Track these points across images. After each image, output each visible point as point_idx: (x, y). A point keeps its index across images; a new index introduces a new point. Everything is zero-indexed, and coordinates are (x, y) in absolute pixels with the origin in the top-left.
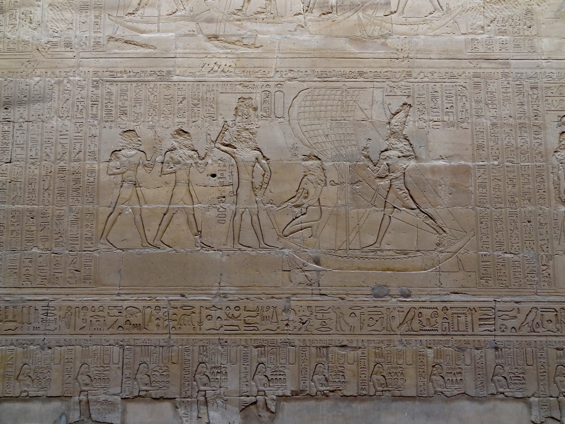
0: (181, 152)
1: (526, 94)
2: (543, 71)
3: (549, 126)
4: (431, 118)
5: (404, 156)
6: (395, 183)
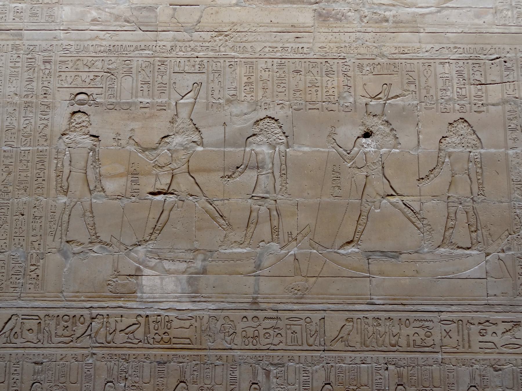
1: (36, 69)
2: (61, 42)
3: (59, 105)
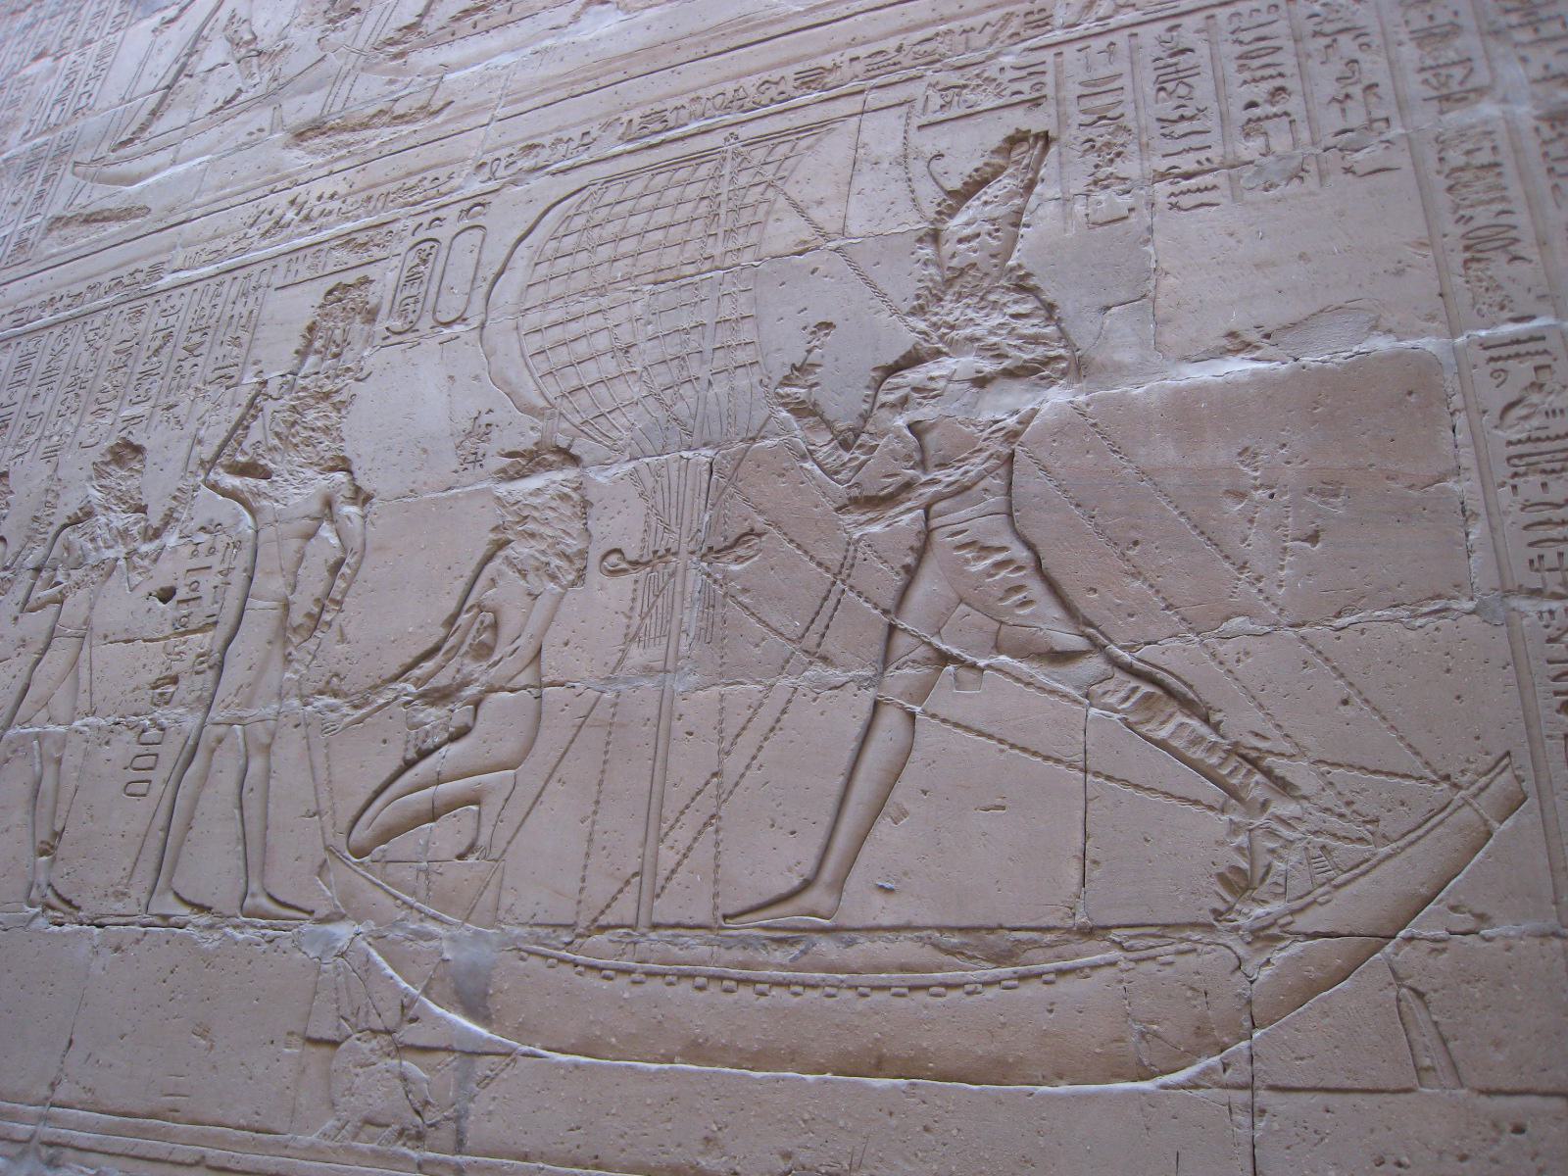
0: (103, 520)
4: (1163, 165)
5: (1009, 374)
6: (956, 517)
